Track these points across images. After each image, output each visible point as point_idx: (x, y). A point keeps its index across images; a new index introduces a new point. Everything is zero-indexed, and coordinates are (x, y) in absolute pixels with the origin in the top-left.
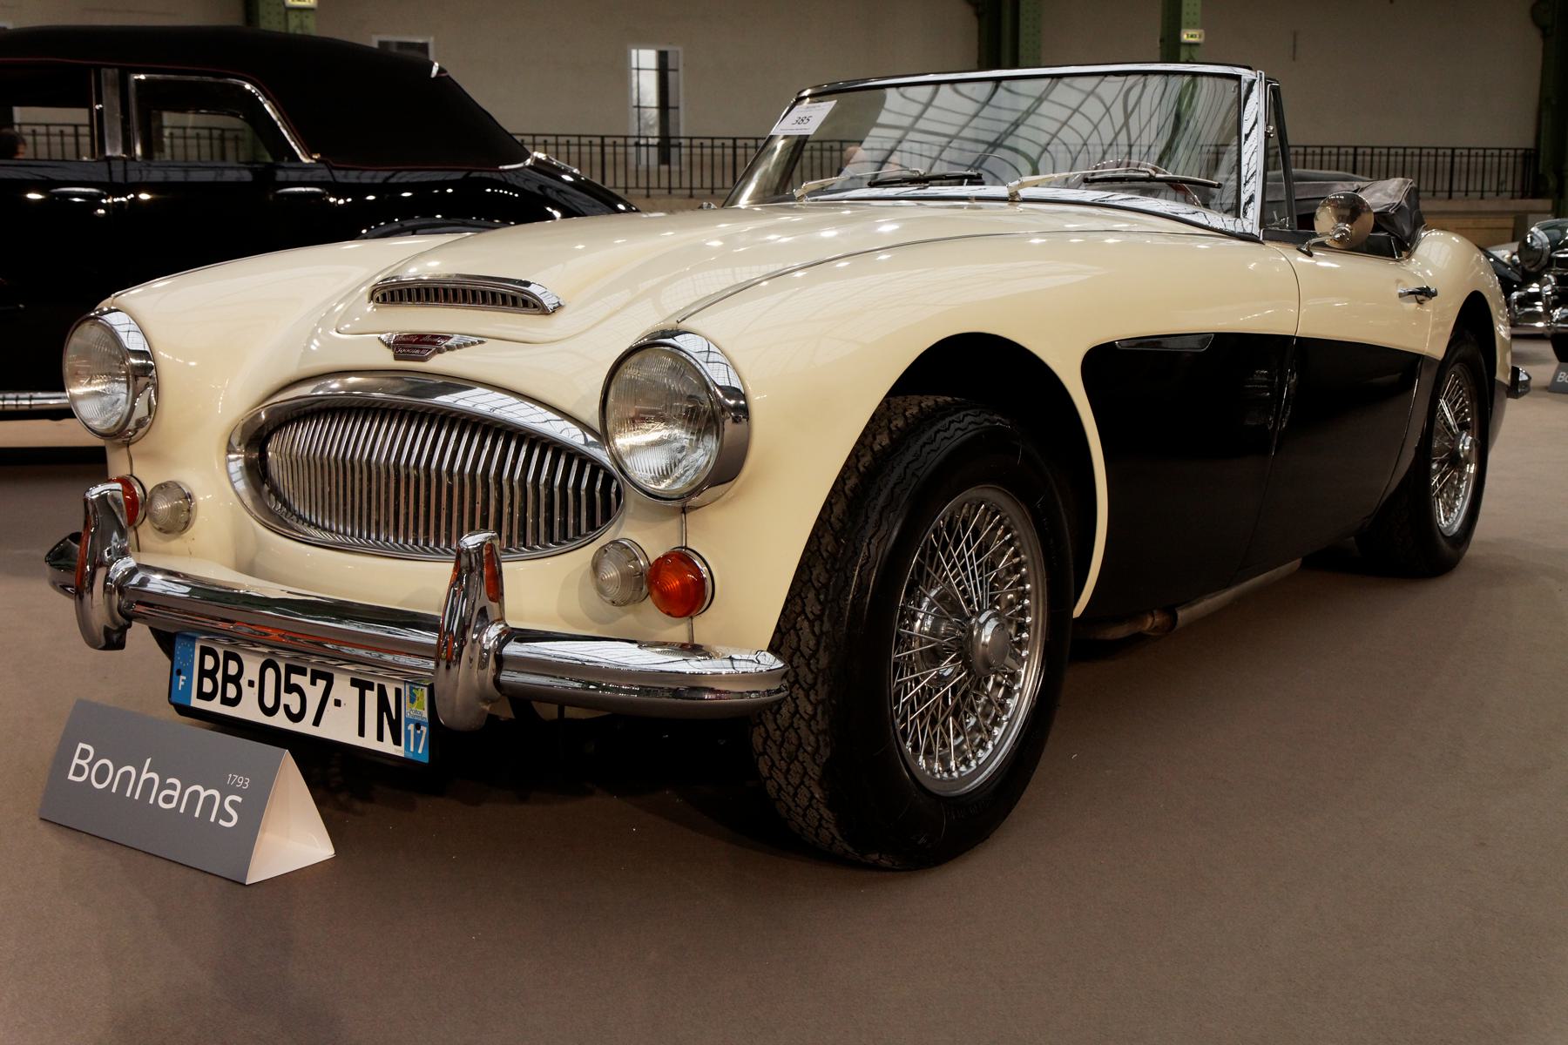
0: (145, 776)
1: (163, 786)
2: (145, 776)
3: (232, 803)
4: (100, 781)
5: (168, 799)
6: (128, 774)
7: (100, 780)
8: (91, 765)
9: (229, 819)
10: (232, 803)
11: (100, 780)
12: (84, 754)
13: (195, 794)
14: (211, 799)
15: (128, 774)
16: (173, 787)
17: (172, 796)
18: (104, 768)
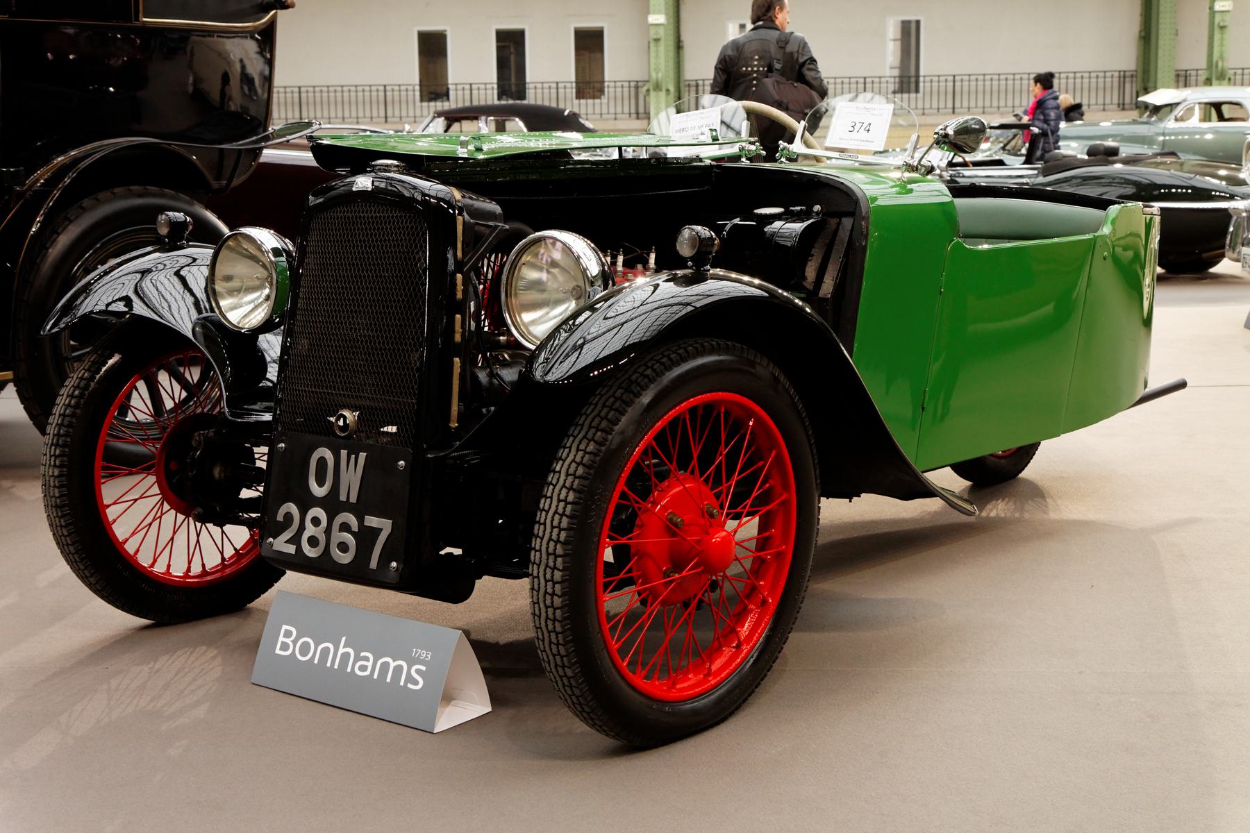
2: (341, 650)
3: (418, 671)
4: (303, 655)
5: (363, 668)
6: (327, 649)
7: (304, 653)
8: (295, 642)
9: (416, 683)
10: (418, 671)
11: (304, 653)
12: (288, 634)
13: (385, 666)
15: (326, 650)
16: (367, 659)
17: (366, 666)
18: (306, 645)
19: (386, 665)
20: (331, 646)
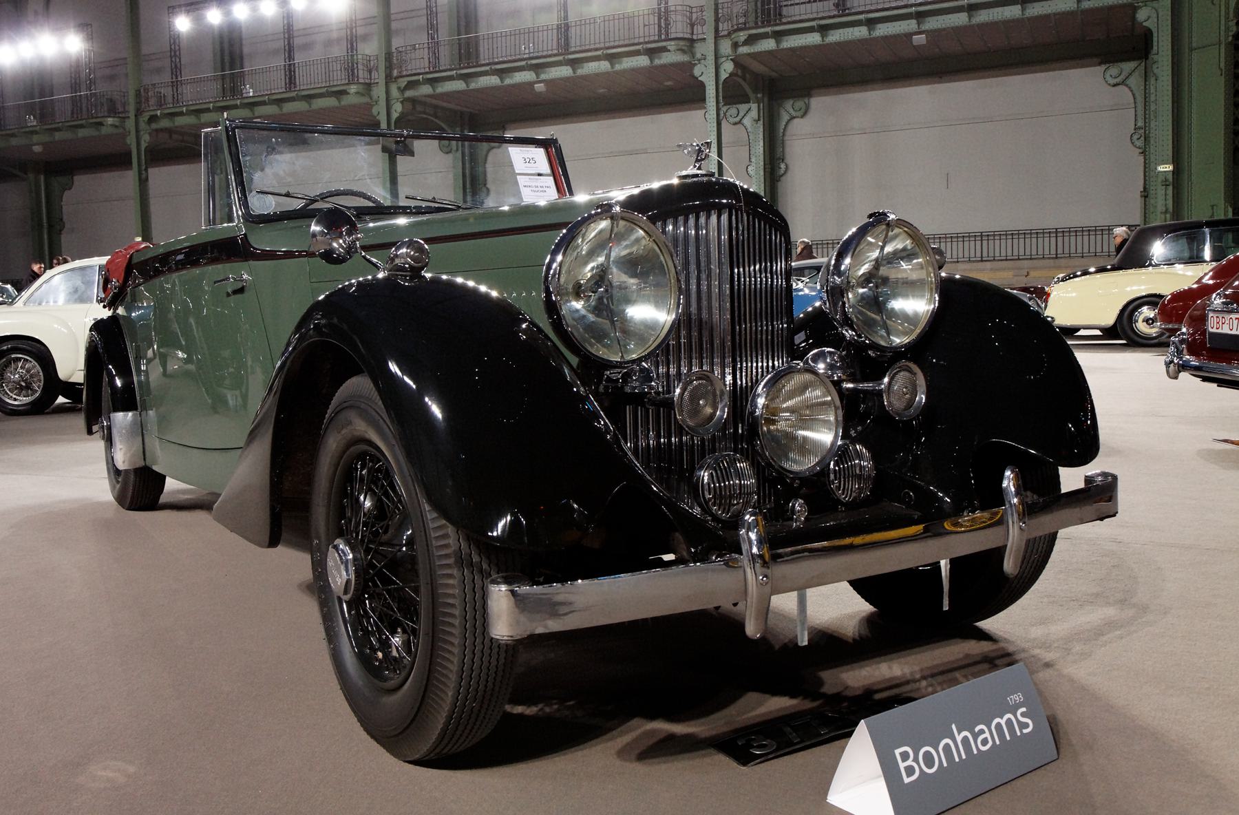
0: (959, 739)
1: (975, 736)
2: (959, 739)
3: (1023, 715)
4: (930, 767)
5: (985, 742)
6: (947, 745)
7: (930, 765)
8: (916, 760)
10: (1023, 715)
11: (930, 763)
13: (999, 726)
14: (1009, 721)
15: (947, 747)
16: (982, 732)
17: (986, 738)
19: (999, 725)
20: (947, 741)
